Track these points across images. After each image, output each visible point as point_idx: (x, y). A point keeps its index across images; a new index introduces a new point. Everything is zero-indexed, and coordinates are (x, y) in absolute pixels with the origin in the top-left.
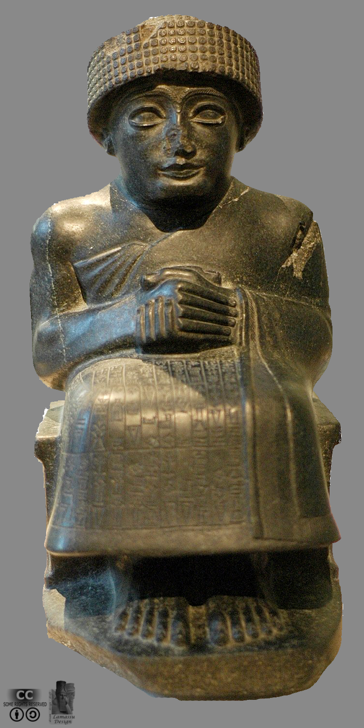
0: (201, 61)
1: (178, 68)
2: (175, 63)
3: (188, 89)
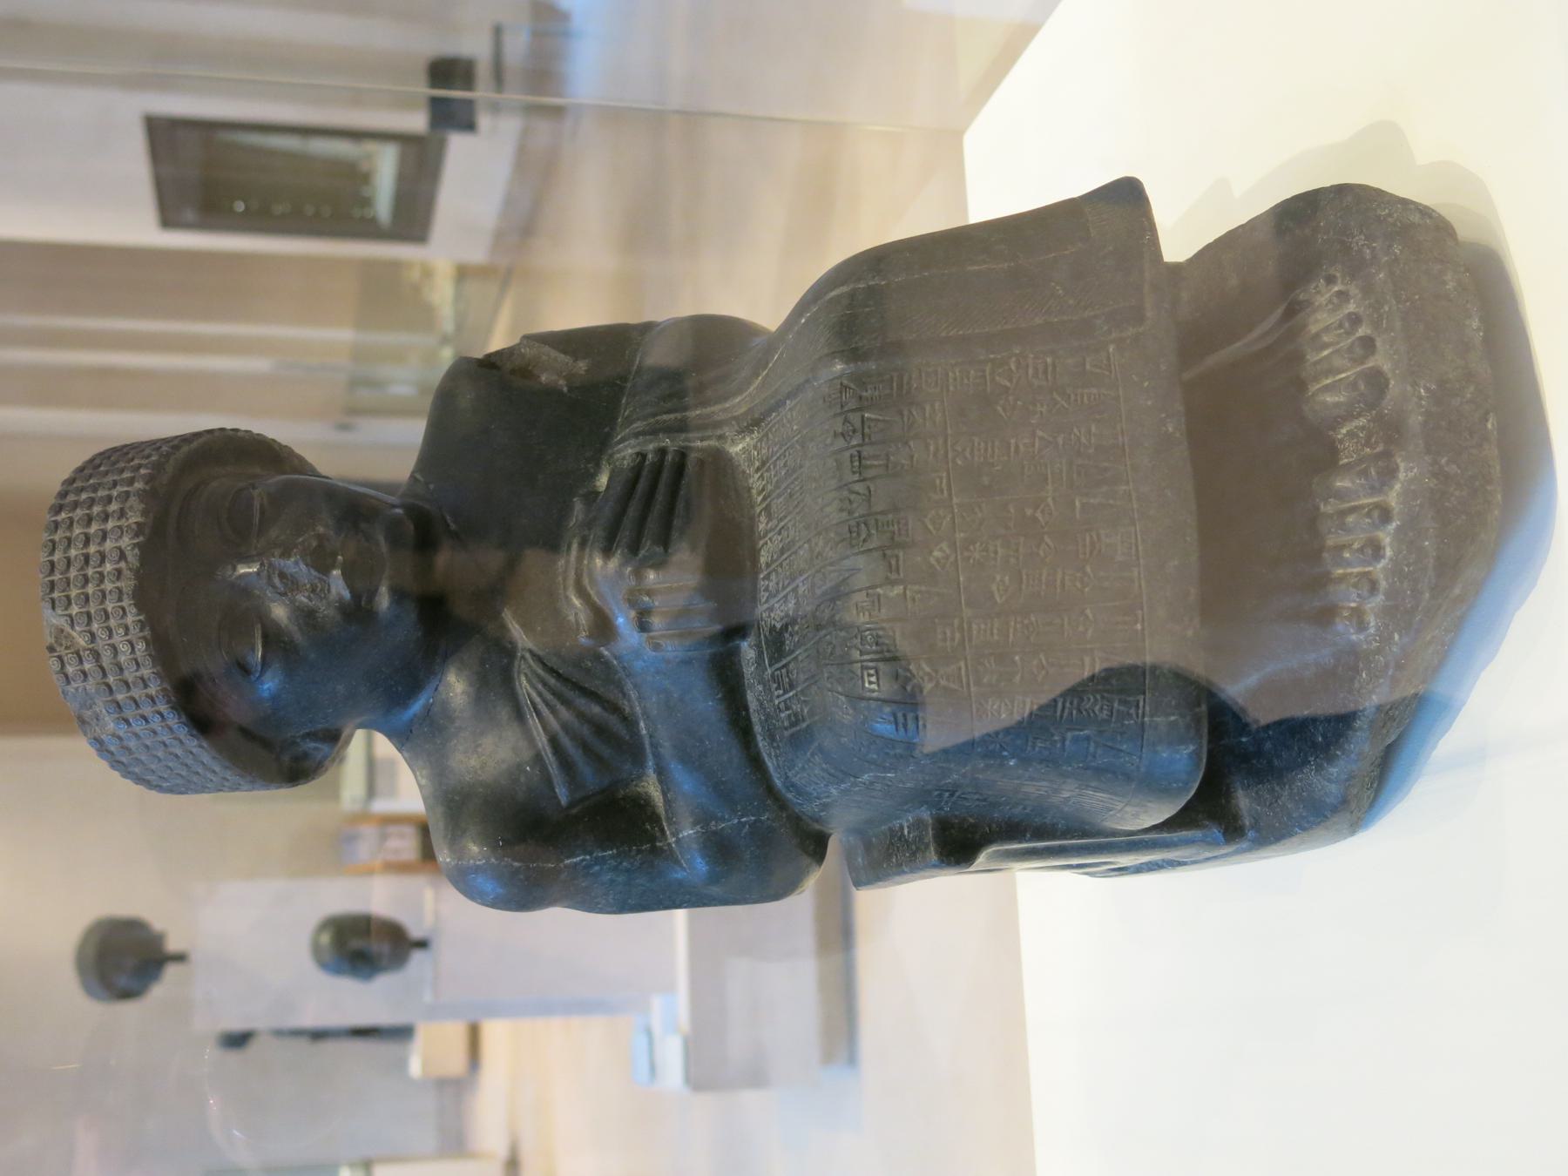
0: (124, 520)
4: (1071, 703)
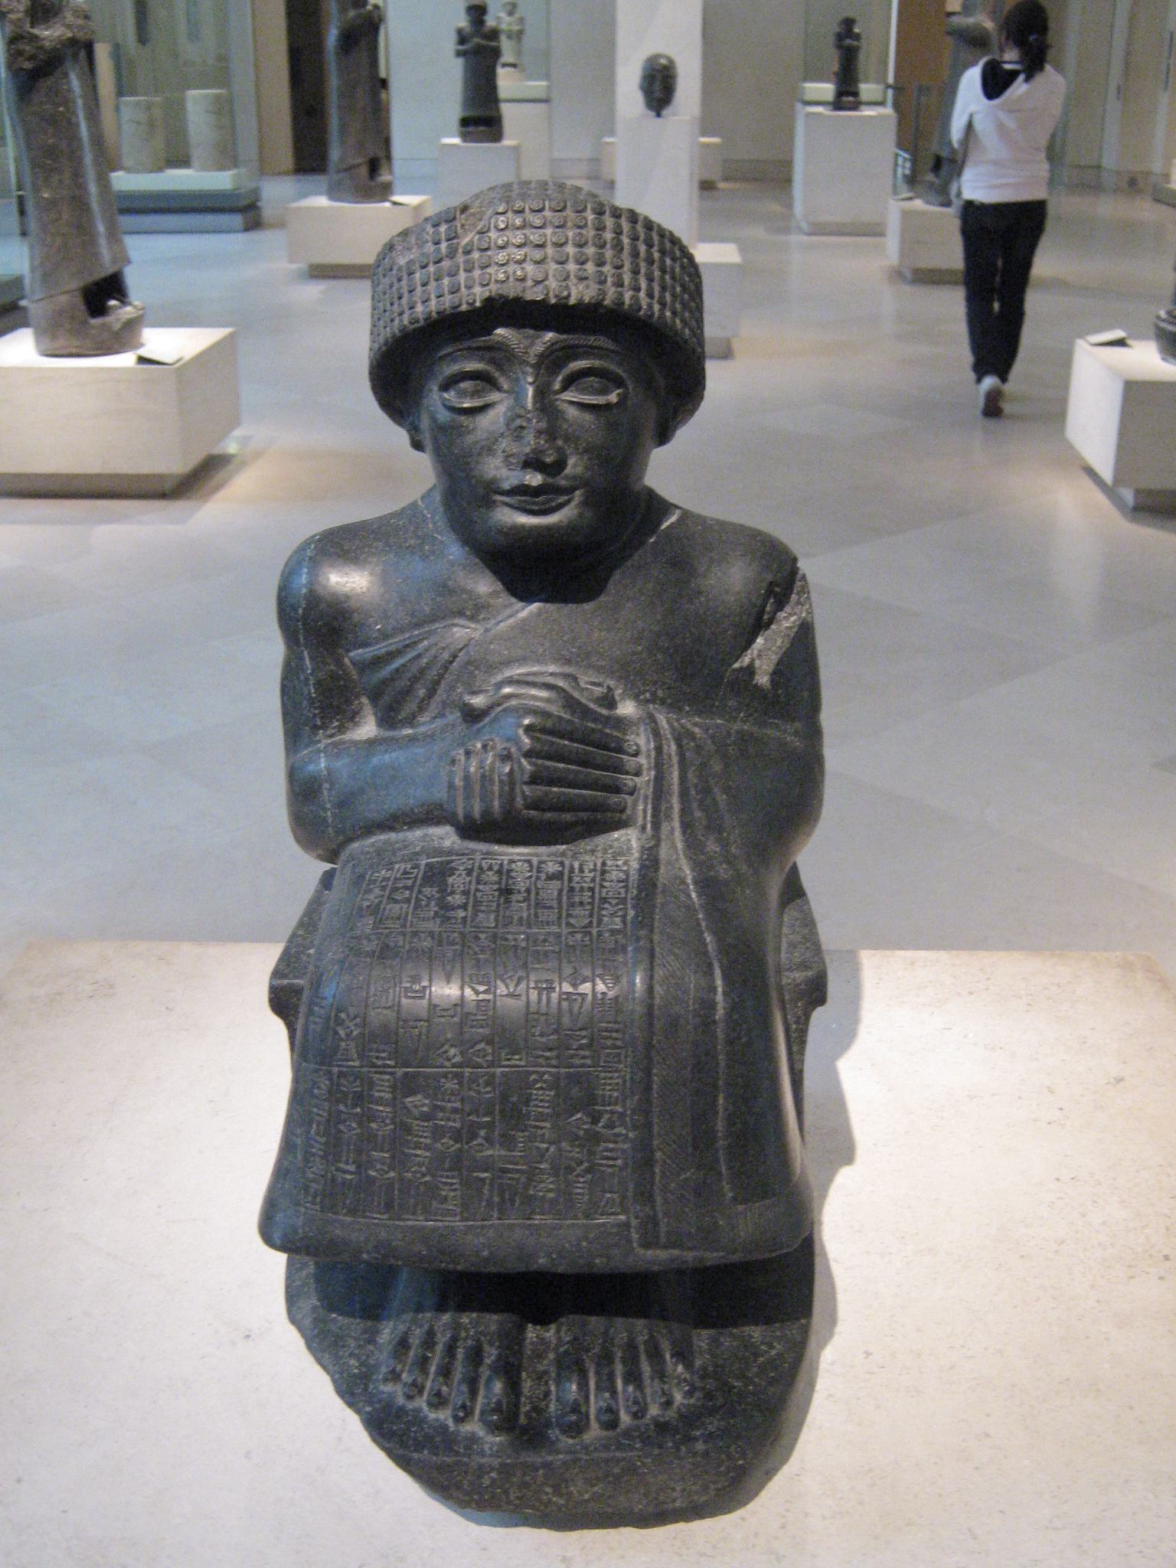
0: (575, 281)
1: (529, 296)
4: (320, 1149)
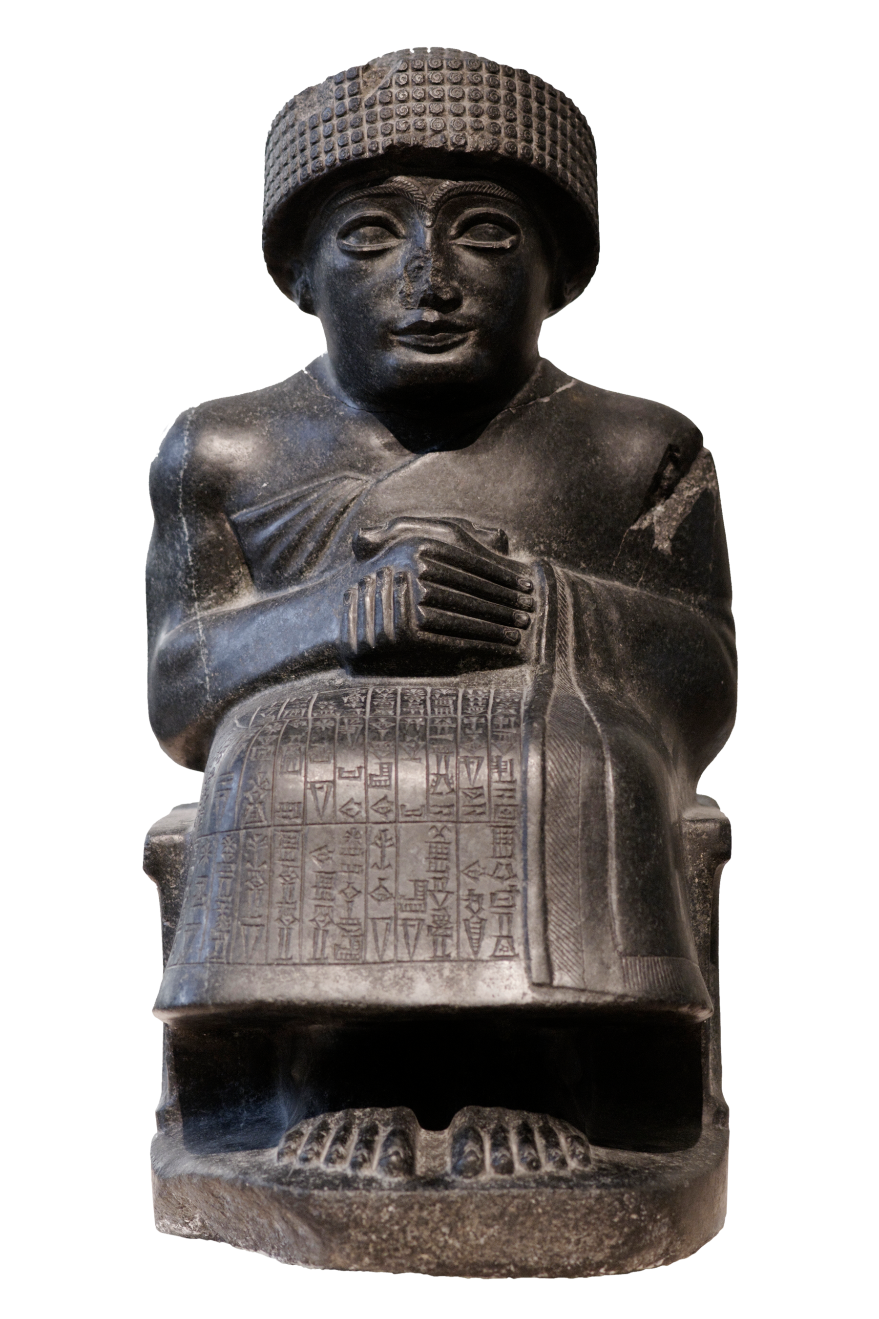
0: (471, 132)
1: (428, 144)
2: (421, 134)
3: (448, 183)
